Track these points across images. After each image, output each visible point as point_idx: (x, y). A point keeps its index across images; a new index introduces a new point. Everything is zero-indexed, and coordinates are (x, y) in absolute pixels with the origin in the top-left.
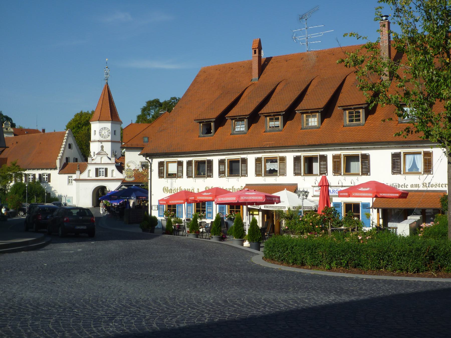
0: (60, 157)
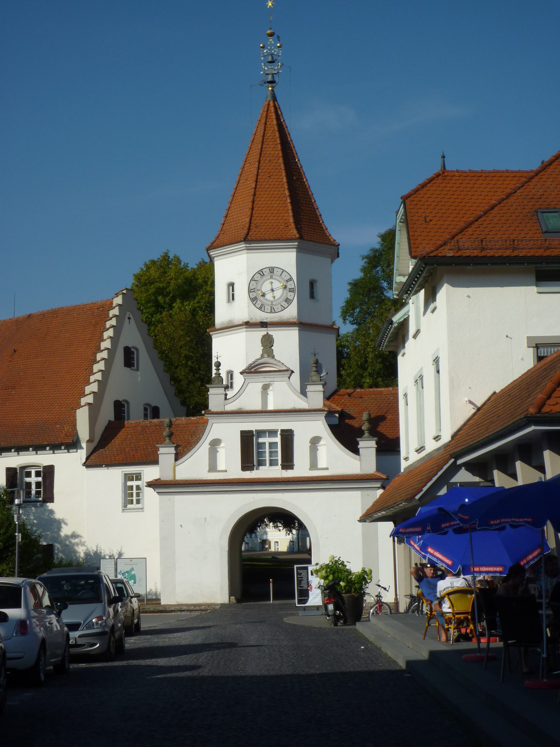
0: (90, 399)
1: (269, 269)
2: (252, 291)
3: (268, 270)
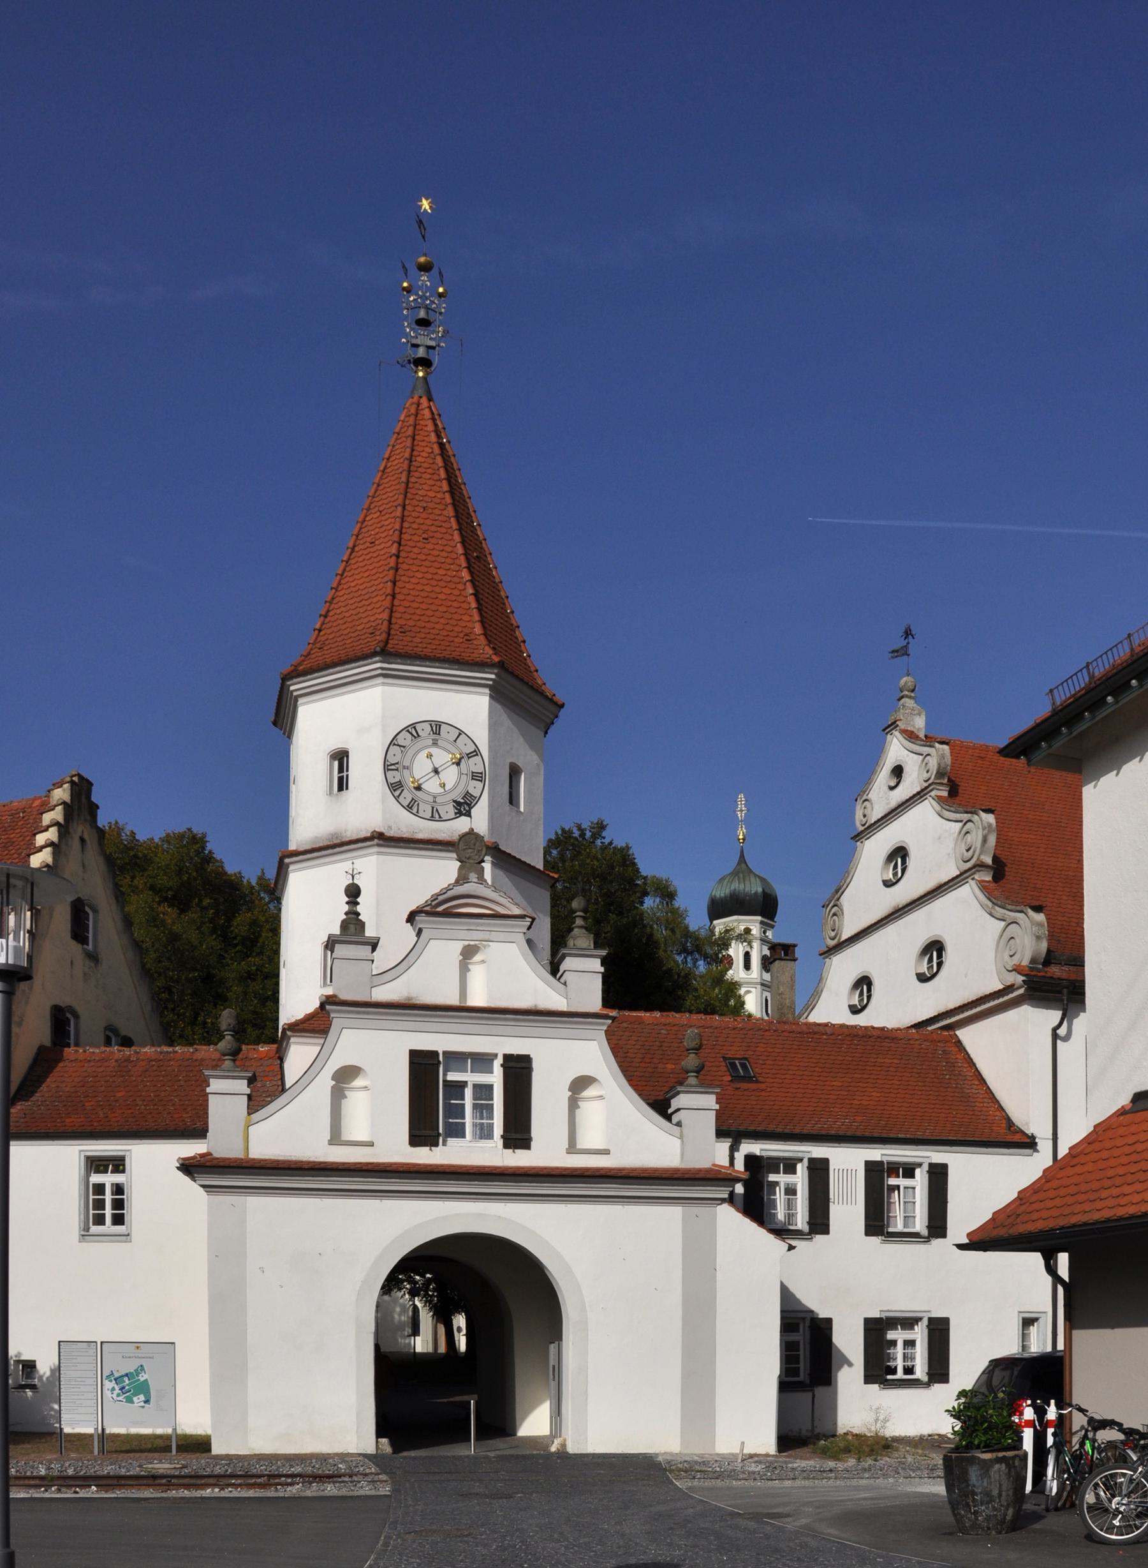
1: (431, 725)
2: (393, 767)
3: (427, 727)
